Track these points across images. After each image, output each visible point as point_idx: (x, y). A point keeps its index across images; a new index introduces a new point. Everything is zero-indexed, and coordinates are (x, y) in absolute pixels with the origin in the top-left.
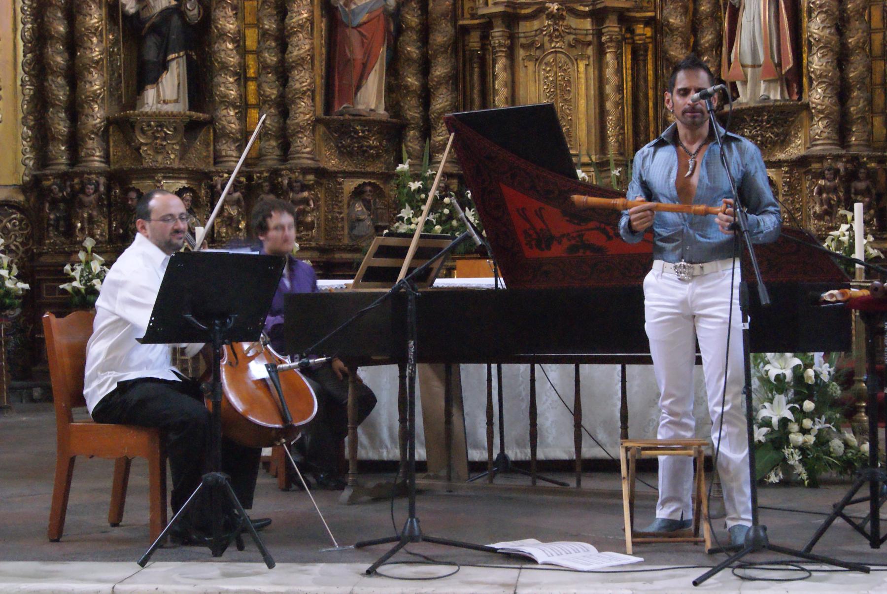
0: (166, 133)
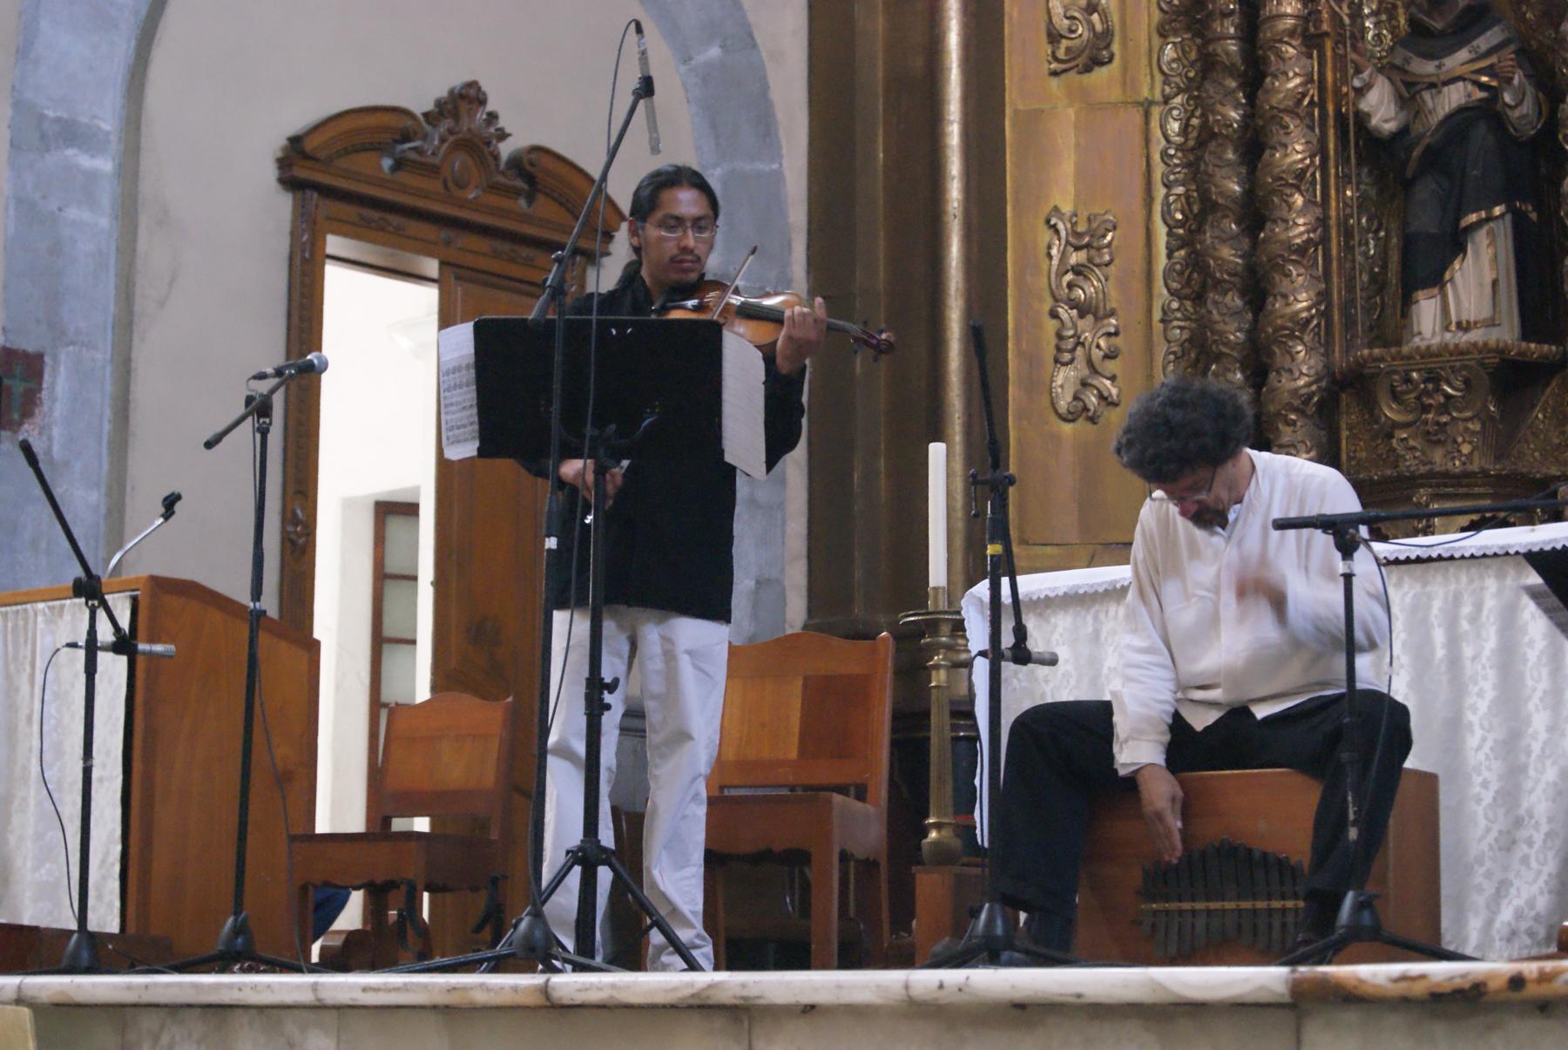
0: (1448, 397)
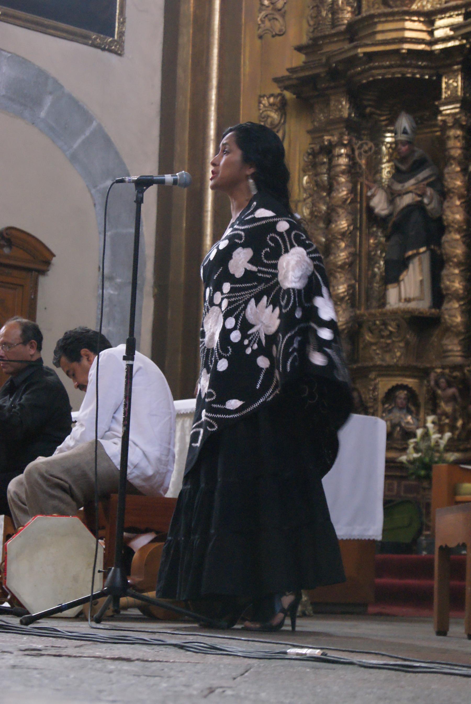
0: (391, 332)
